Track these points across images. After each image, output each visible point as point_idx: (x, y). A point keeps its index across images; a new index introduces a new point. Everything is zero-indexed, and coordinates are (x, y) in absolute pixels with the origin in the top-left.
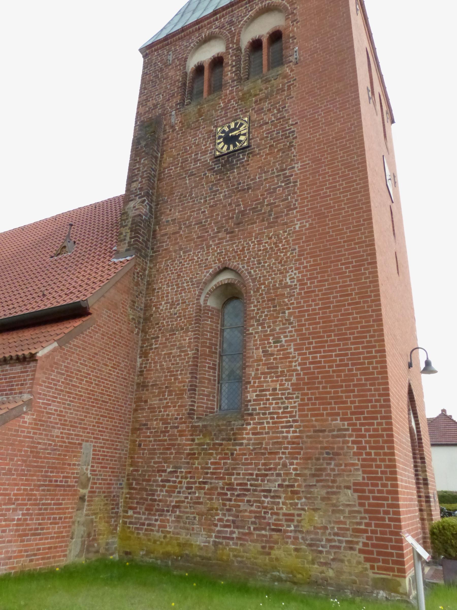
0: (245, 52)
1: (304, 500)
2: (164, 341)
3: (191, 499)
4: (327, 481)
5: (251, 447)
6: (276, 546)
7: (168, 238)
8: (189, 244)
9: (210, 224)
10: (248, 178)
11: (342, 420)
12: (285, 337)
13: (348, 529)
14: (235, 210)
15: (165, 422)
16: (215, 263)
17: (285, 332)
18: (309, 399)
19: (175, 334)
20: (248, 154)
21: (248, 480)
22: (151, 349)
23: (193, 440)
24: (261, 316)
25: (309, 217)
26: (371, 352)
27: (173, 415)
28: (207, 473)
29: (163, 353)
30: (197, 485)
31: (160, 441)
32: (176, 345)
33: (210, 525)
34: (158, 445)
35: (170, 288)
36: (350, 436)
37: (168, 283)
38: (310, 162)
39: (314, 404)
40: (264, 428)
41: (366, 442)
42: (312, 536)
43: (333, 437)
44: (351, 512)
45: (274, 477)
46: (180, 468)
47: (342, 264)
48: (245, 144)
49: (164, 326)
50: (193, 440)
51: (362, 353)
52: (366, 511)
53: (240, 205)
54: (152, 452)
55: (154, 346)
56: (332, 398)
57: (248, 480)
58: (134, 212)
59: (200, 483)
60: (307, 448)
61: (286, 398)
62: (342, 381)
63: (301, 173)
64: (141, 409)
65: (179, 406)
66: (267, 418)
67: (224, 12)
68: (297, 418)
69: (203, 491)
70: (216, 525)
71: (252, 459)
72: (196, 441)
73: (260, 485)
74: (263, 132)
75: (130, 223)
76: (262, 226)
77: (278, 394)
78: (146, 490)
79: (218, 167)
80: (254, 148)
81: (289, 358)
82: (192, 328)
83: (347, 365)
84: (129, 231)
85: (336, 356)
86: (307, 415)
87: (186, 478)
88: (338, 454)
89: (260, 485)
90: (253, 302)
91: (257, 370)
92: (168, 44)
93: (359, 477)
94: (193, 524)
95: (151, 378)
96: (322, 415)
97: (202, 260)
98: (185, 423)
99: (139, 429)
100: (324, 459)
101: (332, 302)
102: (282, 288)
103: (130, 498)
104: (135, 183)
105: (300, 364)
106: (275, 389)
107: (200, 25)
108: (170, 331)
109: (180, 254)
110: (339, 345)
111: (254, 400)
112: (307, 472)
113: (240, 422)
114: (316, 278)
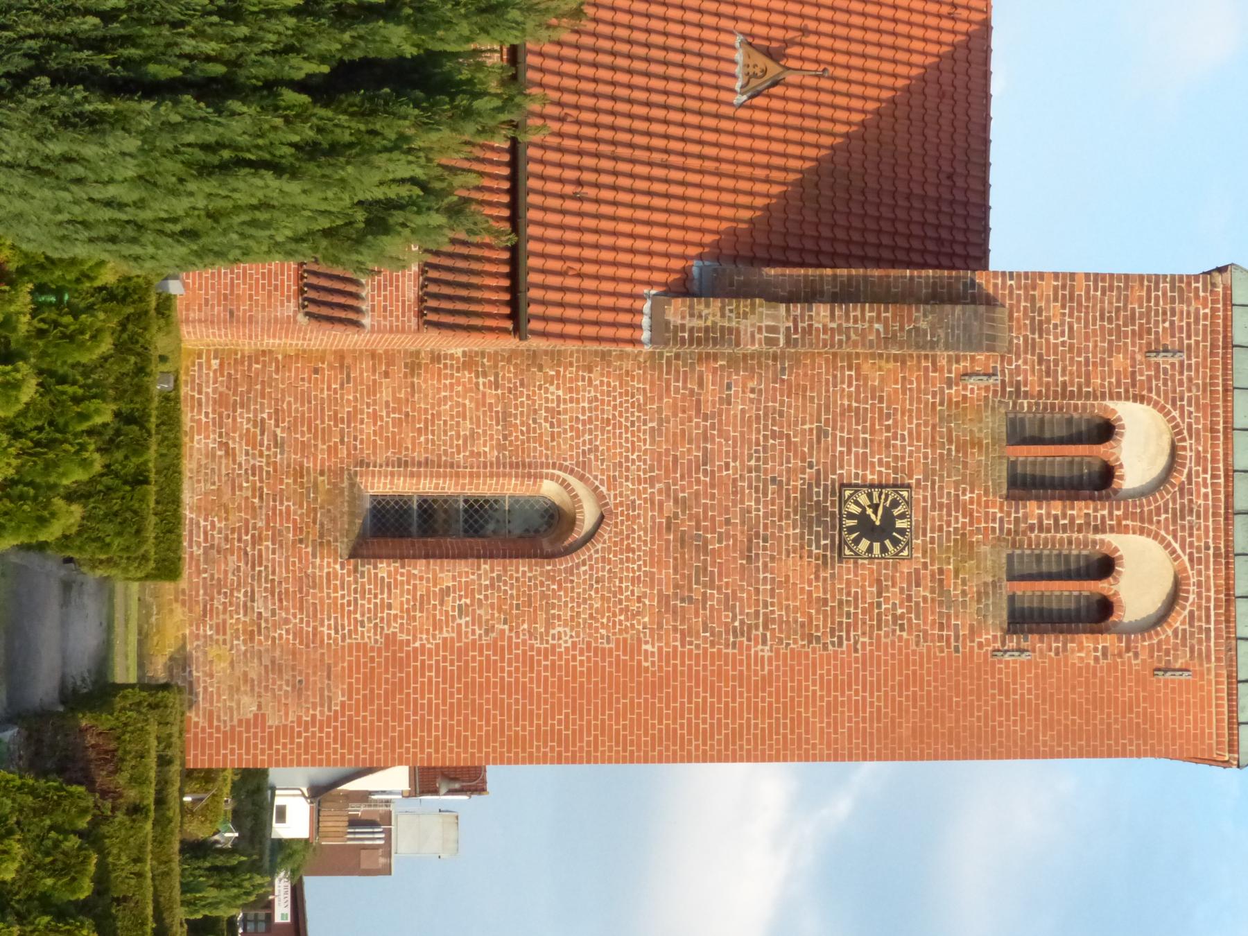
0: (1094, 542)
1: (243, 648)
2: (488, 401)
3: (239, 475)
4: (267, 681)
5: (310, 571)
6: (186, 610)
7: (692, 391)
8: (667, 441)
9: (698, 481)
10: (773, 558)
11: (343, 704)
12: (467, 623)
13: (212, 704)
14: (713, 531)
15: (351, 417)
16: (615, 498)
17: (473, 624)
18: (372, 659)
19: (498, 424)
20: (825, 556)
21: (266, 567)
22: (477, 377)
23: (322, 473)
24: (505, 583)
25: (660, 667)
26: (429, 747)
27: (362, 431)
28: (274, 500)
29: (467, 402)
30: (258, 484)
31: (323, 409)
32: (478, 427)
33: (206, 509)
34: (316, 405)
35: (586, 405)
36: (322, 713)
37: (596, 399)
38: (766, 672)
39: (365, 664)
40: (336, 591)
41: (314, 733)
42: (201, 660)
43: (322, 690)
44: (231, 708)
45: (270, 607)
46: (282, 453)
47: (567, 715)
48: (847, 552)
49: (516, 399)
50: (322, 473)
51: (429, 735)
52: (233, 727)
53: (720, 542)
54: (304, 398)
55: (481, 380)
56: (372, 691)
57: (266, 567)
58: (749, 330)
59: (261, 488)
60: (308, 653)
61: (376, 625)
62: (394, 706)
63: (749, 657)
64: (374, 365)
65: (375, 441)
66: (349, 595)
67: (1222, 496)
68: (348, 641)
69: (250, 494)
70: (206, 520)
71: (294, 571)
72: (320, 479)
73: (260, 586)
74: (863, 587)
75: (726, 324)
76: (667, 584)
77: (382, 612)
78: (249, 392)
79: (818, 494)
80: (833, 568)
81: (434, 629)
82: (504, 455)
83: (415, 714)
84: (709, 323)
85: (430, 700)
86: (350, 655)
87: (268, 464)
88: (299, 696)
89: (260, 586)
90: (531, 570)
91: (421, 579)
92: (1214, 346)
93: (272, 721)
94: (206, 481)
95: (426, 381)
96: (350, 677)
97: (628, 469)
98: (349, 455)
99: (342, 366)
100: (294, 676)
101: (510, 697)
102: (547, 620)
103: (236, 360)
104: (828, 313)
105: (423, 646)
106: (390, 607)
107: (1221, 435)
108: (504, 412)
109: (652, 420)
110: (444, 704)
111: (376, 575)
112: (277, 653)
113: (346, 553)
114: (553, 676)
